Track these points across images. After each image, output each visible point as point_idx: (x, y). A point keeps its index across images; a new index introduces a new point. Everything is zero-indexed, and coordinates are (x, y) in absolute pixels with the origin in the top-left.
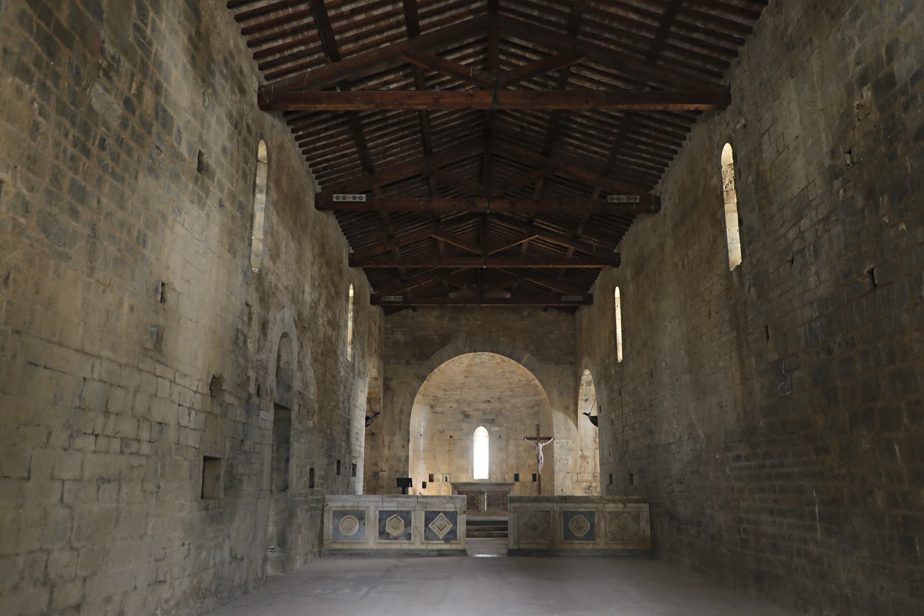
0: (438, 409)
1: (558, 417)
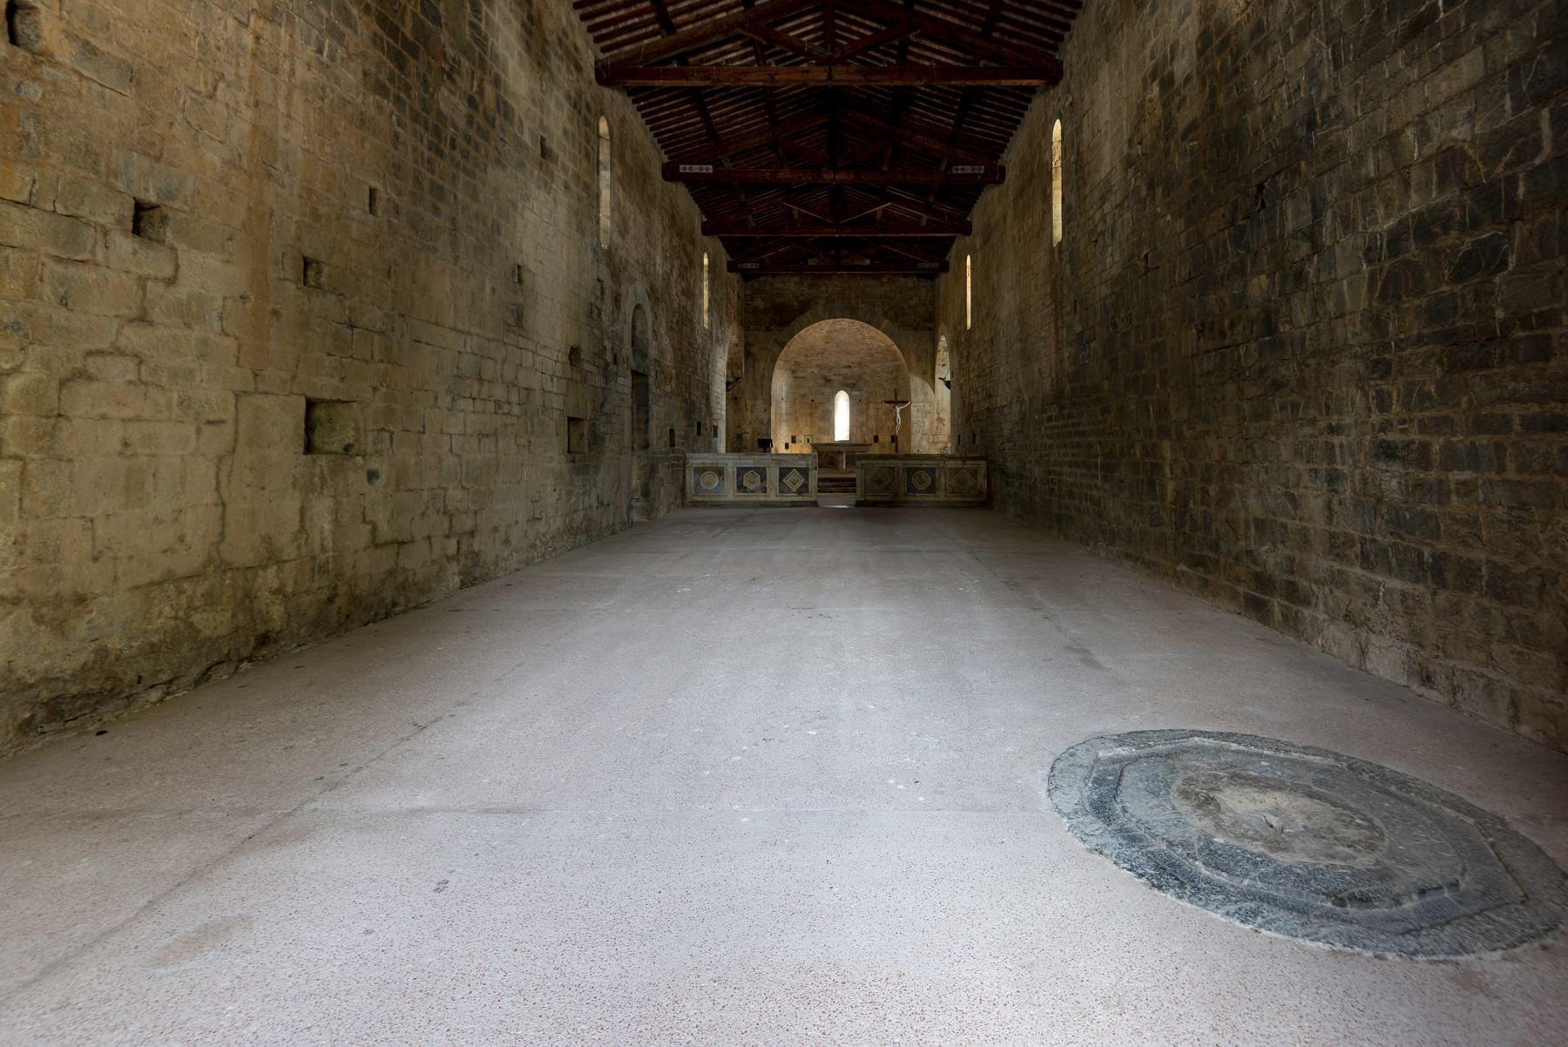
0: (799, 374)
1: (916, 382)
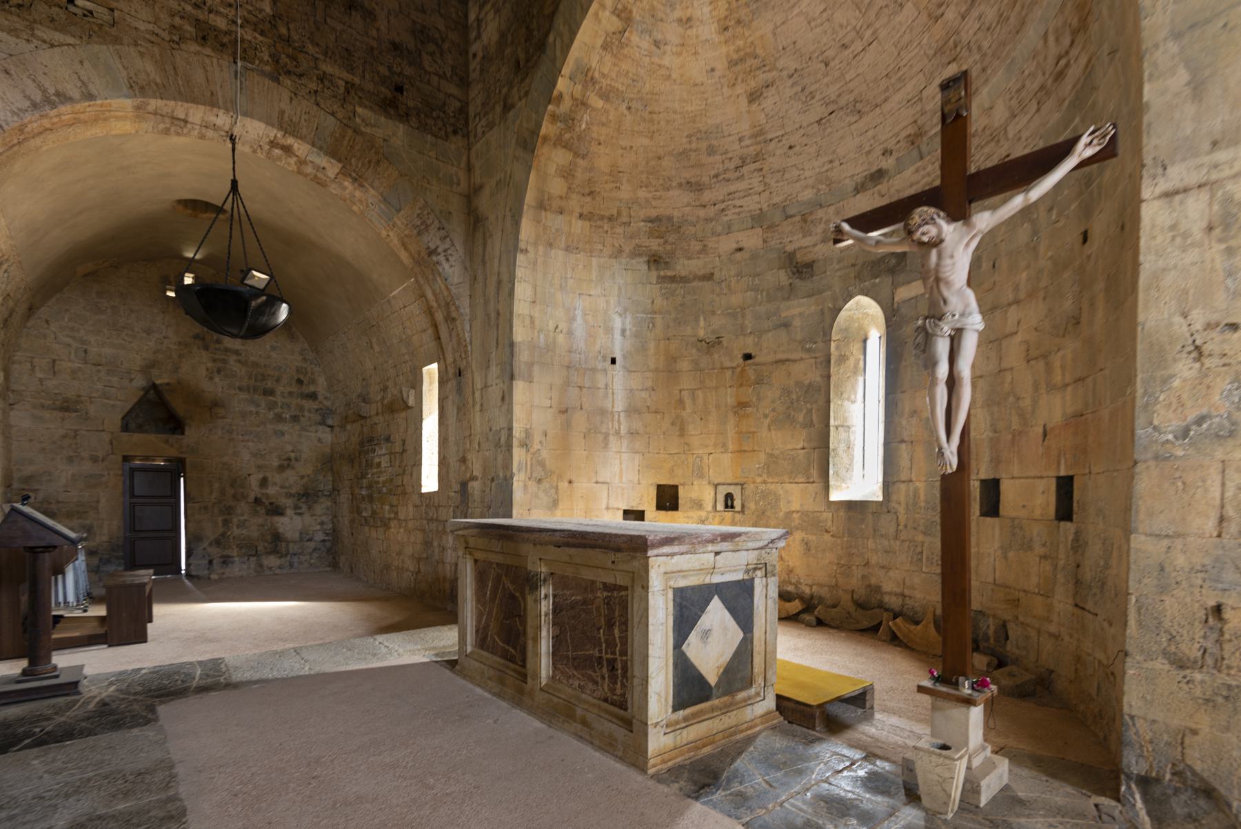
0: (684, 266)
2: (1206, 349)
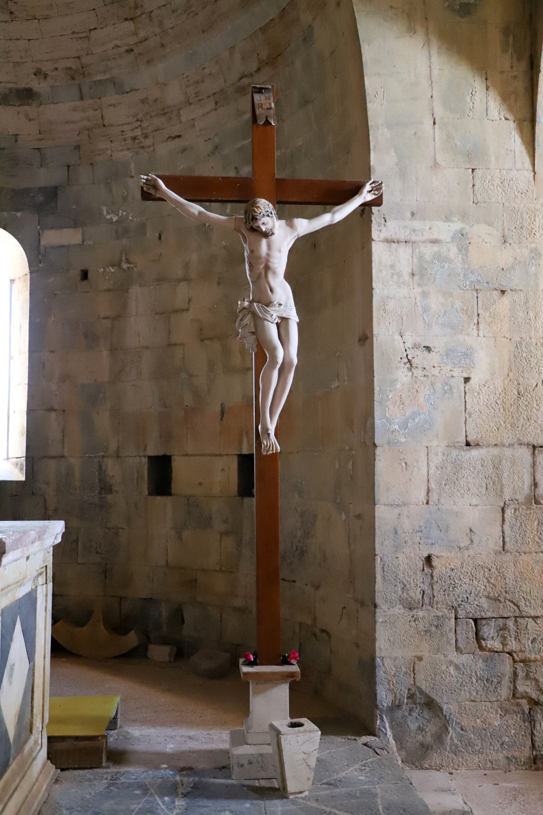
2: (415, 362)
